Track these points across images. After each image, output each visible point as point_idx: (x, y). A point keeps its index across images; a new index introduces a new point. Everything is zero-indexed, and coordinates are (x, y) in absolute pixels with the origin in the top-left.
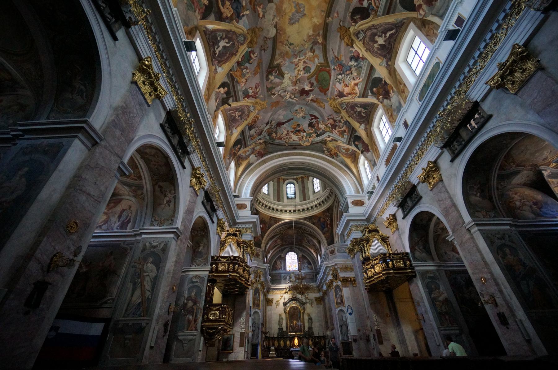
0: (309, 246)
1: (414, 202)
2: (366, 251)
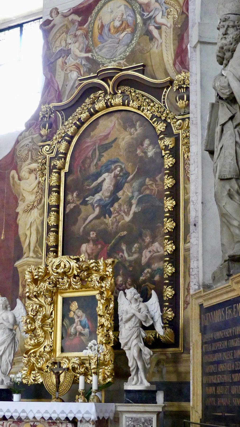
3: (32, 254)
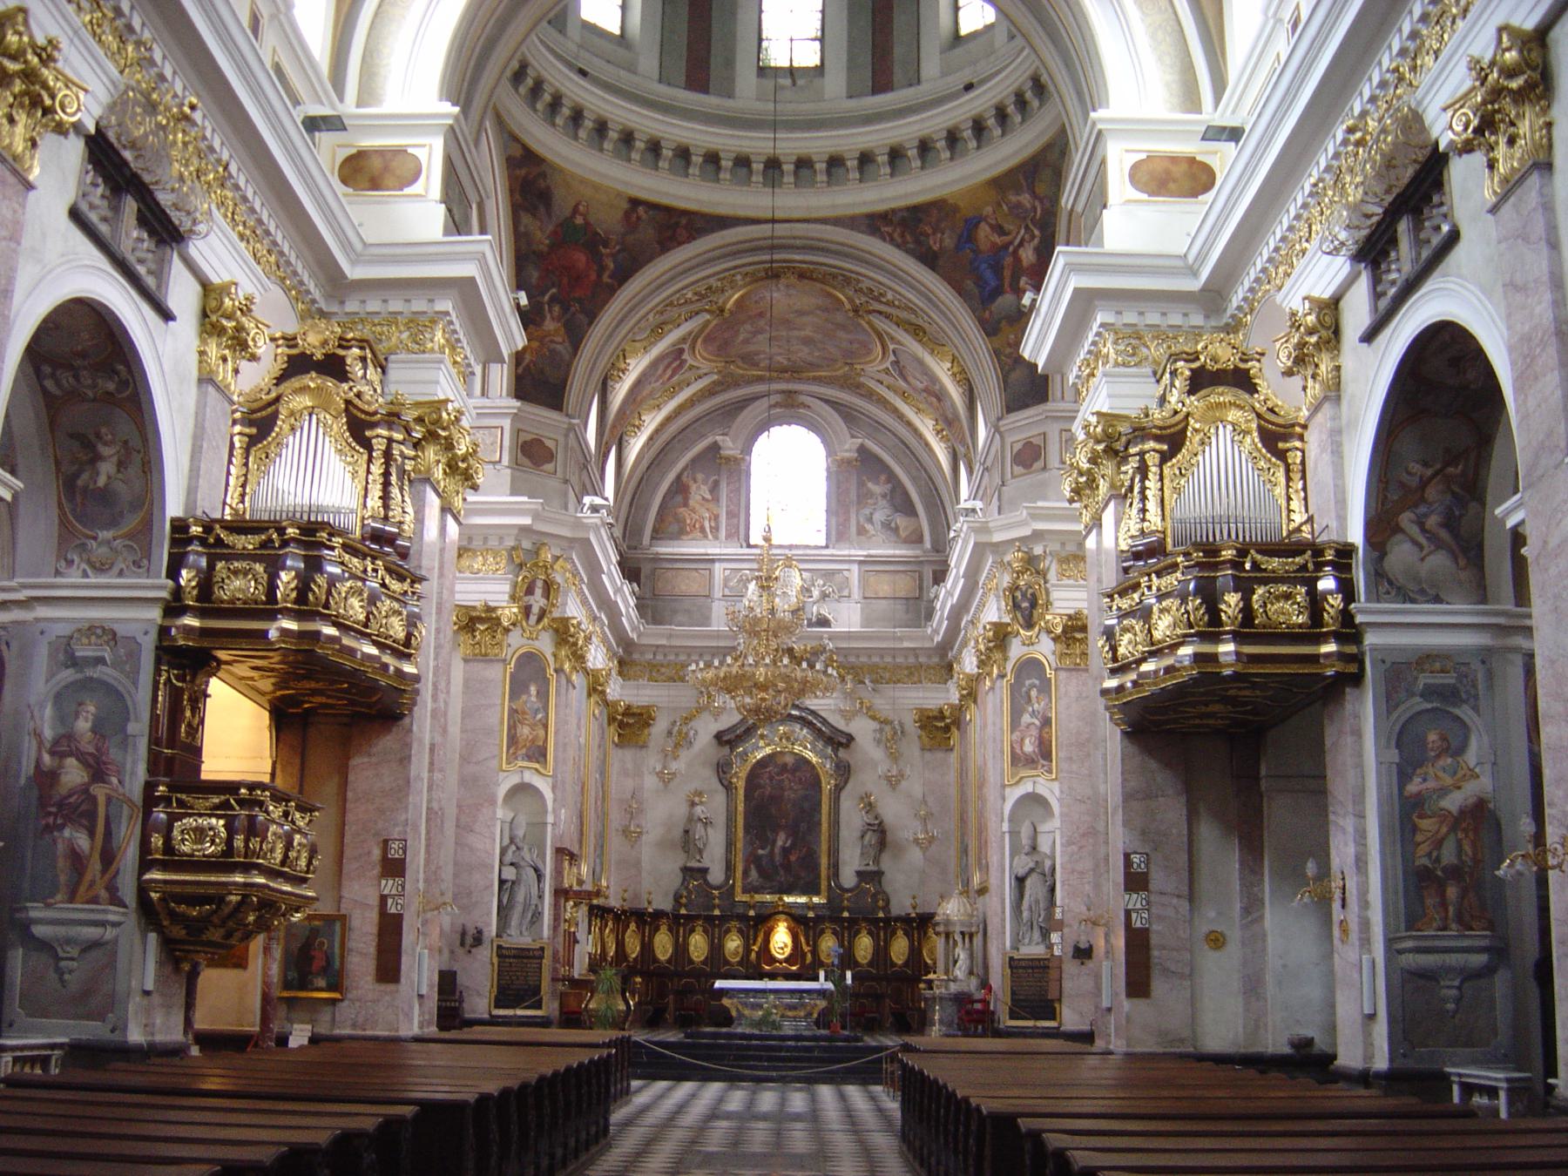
0: (903, 395)
1: (1426, 253)
2: (1152, 505)
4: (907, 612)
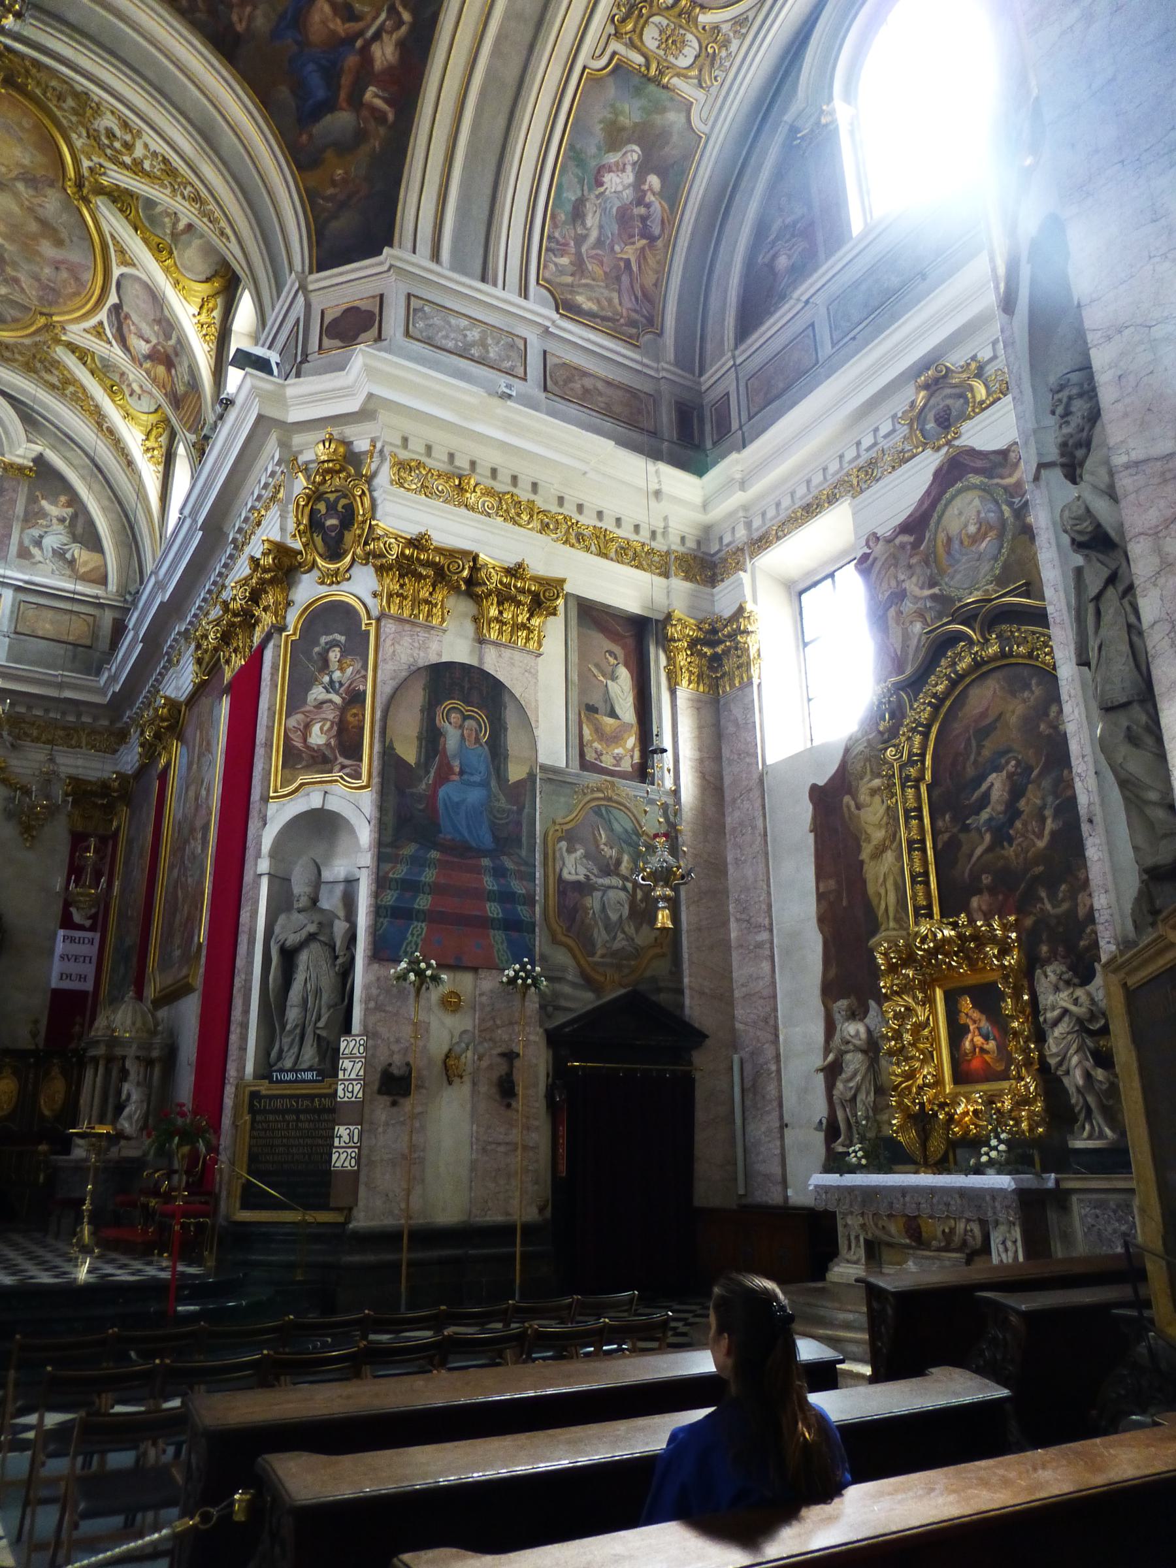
3: (892, 924)
4: (74, 657)
